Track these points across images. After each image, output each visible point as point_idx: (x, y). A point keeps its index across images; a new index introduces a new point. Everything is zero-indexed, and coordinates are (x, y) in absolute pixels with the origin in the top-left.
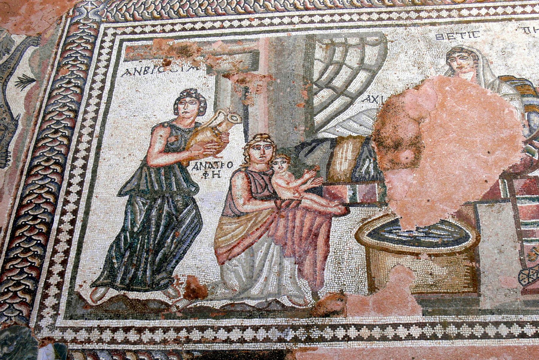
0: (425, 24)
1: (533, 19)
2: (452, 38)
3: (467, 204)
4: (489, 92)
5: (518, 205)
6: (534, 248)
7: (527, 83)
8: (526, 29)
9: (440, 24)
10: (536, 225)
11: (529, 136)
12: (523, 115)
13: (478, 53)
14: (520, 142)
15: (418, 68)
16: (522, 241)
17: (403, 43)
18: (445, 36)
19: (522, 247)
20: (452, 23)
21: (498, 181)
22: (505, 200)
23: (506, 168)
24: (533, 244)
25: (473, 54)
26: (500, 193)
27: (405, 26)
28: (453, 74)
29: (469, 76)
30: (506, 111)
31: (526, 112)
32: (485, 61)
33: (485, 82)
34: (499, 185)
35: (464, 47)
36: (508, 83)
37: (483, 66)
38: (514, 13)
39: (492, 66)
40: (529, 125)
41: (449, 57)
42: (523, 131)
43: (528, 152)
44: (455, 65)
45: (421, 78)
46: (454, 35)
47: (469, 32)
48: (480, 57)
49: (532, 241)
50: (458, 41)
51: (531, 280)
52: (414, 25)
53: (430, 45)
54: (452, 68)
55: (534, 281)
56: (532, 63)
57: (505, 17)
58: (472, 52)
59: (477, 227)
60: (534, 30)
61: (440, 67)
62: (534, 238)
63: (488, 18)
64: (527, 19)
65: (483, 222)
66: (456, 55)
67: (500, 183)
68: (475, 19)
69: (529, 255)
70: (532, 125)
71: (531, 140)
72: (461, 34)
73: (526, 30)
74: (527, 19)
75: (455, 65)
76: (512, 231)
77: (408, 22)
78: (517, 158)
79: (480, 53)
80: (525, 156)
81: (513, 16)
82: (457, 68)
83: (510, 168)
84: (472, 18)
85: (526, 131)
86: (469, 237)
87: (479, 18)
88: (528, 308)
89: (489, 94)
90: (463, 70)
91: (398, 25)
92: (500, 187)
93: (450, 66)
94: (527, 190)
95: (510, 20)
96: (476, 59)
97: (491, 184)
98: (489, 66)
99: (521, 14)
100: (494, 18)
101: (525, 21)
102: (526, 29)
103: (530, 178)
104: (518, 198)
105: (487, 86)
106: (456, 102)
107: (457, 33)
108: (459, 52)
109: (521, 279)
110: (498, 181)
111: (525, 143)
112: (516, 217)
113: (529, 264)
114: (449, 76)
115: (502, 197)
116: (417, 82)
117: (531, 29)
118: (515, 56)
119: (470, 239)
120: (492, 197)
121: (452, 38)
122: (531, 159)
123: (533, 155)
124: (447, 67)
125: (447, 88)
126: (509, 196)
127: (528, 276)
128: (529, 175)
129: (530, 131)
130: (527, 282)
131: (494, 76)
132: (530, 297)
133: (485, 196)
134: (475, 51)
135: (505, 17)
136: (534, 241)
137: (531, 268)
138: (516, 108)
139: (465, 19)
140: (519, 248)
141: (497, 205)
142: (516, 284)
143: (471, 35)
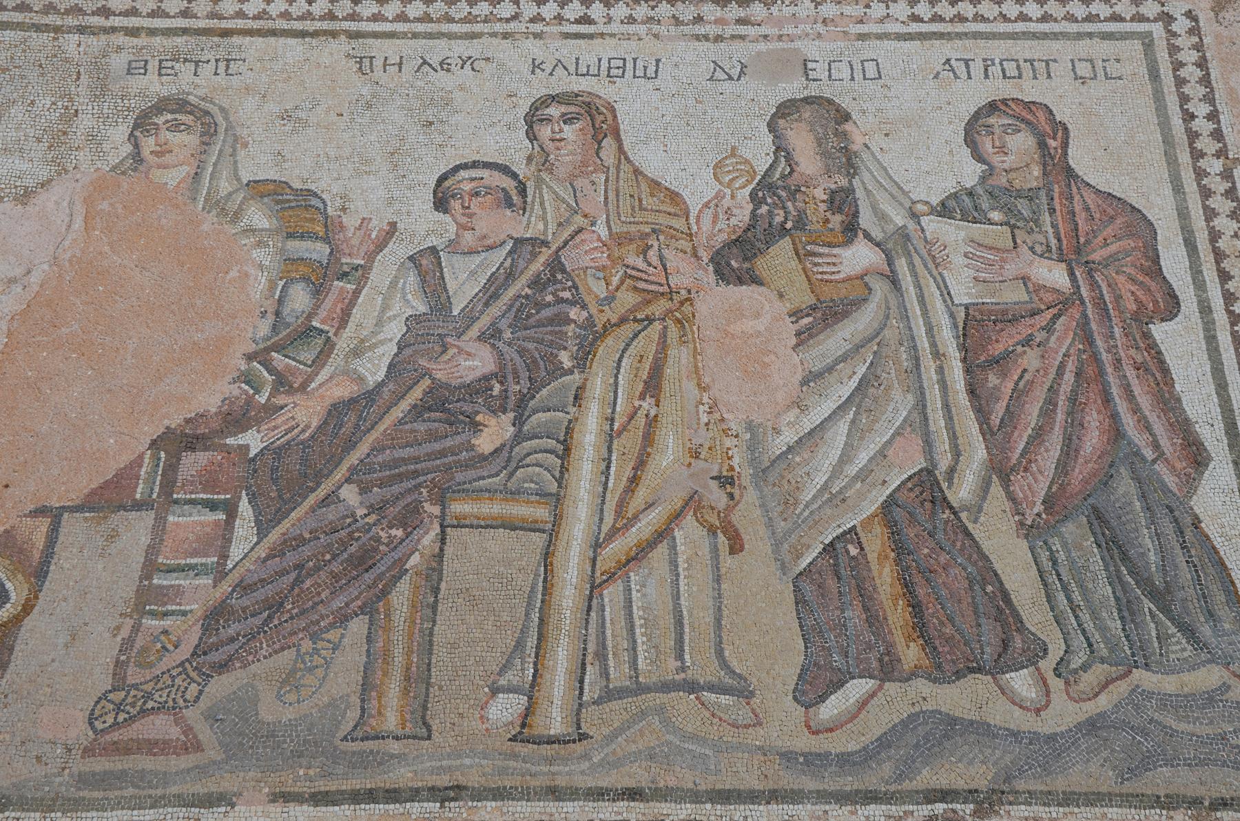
0: (114, 30)
1: (392, 35)
2: (169, 71)
3: (40, 512)
4: (209, 222)
5: (171, 518)
6: (165, 632)
7: (314, 202)
8: (366, 62)
9: (152, 32)
10: (192, 573)
11: (269, 339)
12: (272, 286)
13: (220, 119)
14: (239, 355)
15: (49, 148)
16: (144, 613)
17: (32, 76)
18: (153, 65)
19: (136, 628)
20: (185, 31)
21: (141, 456)
22: (138, 506)
23: (175, 421)
24: (167, 623)
25: (207, 119)
26: (137, 484)
27: (57, 30)
28: (135, 170)
29: (174, 177)
30: (233, 274)
31: (281, 279)
32: (230, 140)
33: (208, 193)
34: (141, 466)
35: (191, 98)
36: (266, 200)
37: (221, 151)
38: (353, 17)
39: (242, 153)
40: (277, 314)
41: (143, 123)
42: (255, 327)
43: (247, 383)
44: (149, 144)
45: (44, 174)
46: (177, 66)
47: (217, 61)
48: (221, 130)
49: (166, 614)
50: (185, 81)
51: (121, 718)
52: (81, 30)
53: (101, 90)
54: (139, 153)
55: (131, 719)
56: (347, 151)
57: (325, 25)
58: (207, 113)
59: (41, 573)
60: (385, 66)
61: (106, 146)
62: (174, 607)
63: (282, 24)
64: (375, 35)
65: (65, 562)
66: (160, 120)
67: (147, 461)
68: (250, 24)
69: (144, 650)
70: (286, 311)
71: (267, 350)
72: (197, 63)
73: (363, 64)
74: (375, 35)
75: (149, 144)
76: (126, 590)
77: (71, 21)
78: (211, 398)
79: (226, 119)
80: (236, 392)
81: (346, 25)
82: (152, 152)
83: (188, 421)
84: (240, 23)
85: (264, 328)
86: (7, 599)
87: (256, 25)
88: (85, 793)
89: (206, 227)
90: (168, 159)
91: (38, 28)
92: (144, 469)
93: (136, 146)
94: (209, 481)
95: (334, 34)
96: (209, 132)
97: (125, 459)
98: (233, 155)
99: (368, 20)
100: (298, 25)
101: (370, 41)
102: (366, 62)
103: (228, 450)
104: (176, 502)
105: (217, 205)
106: (111, 244)
107: (186, 60)
108: (173, 112)
109: (97, 713)
110: (141, 456)
111: (250, 357)
112: (152, 550)
113: (134, 675)
114: (123, 173)
115: (138, 496)
116: (29, 182)
117: (378, 63)
118: (310, 131)
119: (8, 605)
120: (109, 499)
121: (169, 71)
122: (249, 401)
123: (257, 391)
124: (128, 148)
125: (105, 206)
126: (155, 496)
127: (118, 708)
128: (228, 441)
129: (274, 328)
130: (110, 721)
131: (238, 180)
132: (101, 764)
133: (93, 493)
134: (215, 110)
135: (325, 25)
136: (173, 613)
137: (135, 686)
138: (261, 267)
139: (224, 24)
140: (125, 633)
141: (116, 519)
142: (79, 732)
143: (222, 65)
